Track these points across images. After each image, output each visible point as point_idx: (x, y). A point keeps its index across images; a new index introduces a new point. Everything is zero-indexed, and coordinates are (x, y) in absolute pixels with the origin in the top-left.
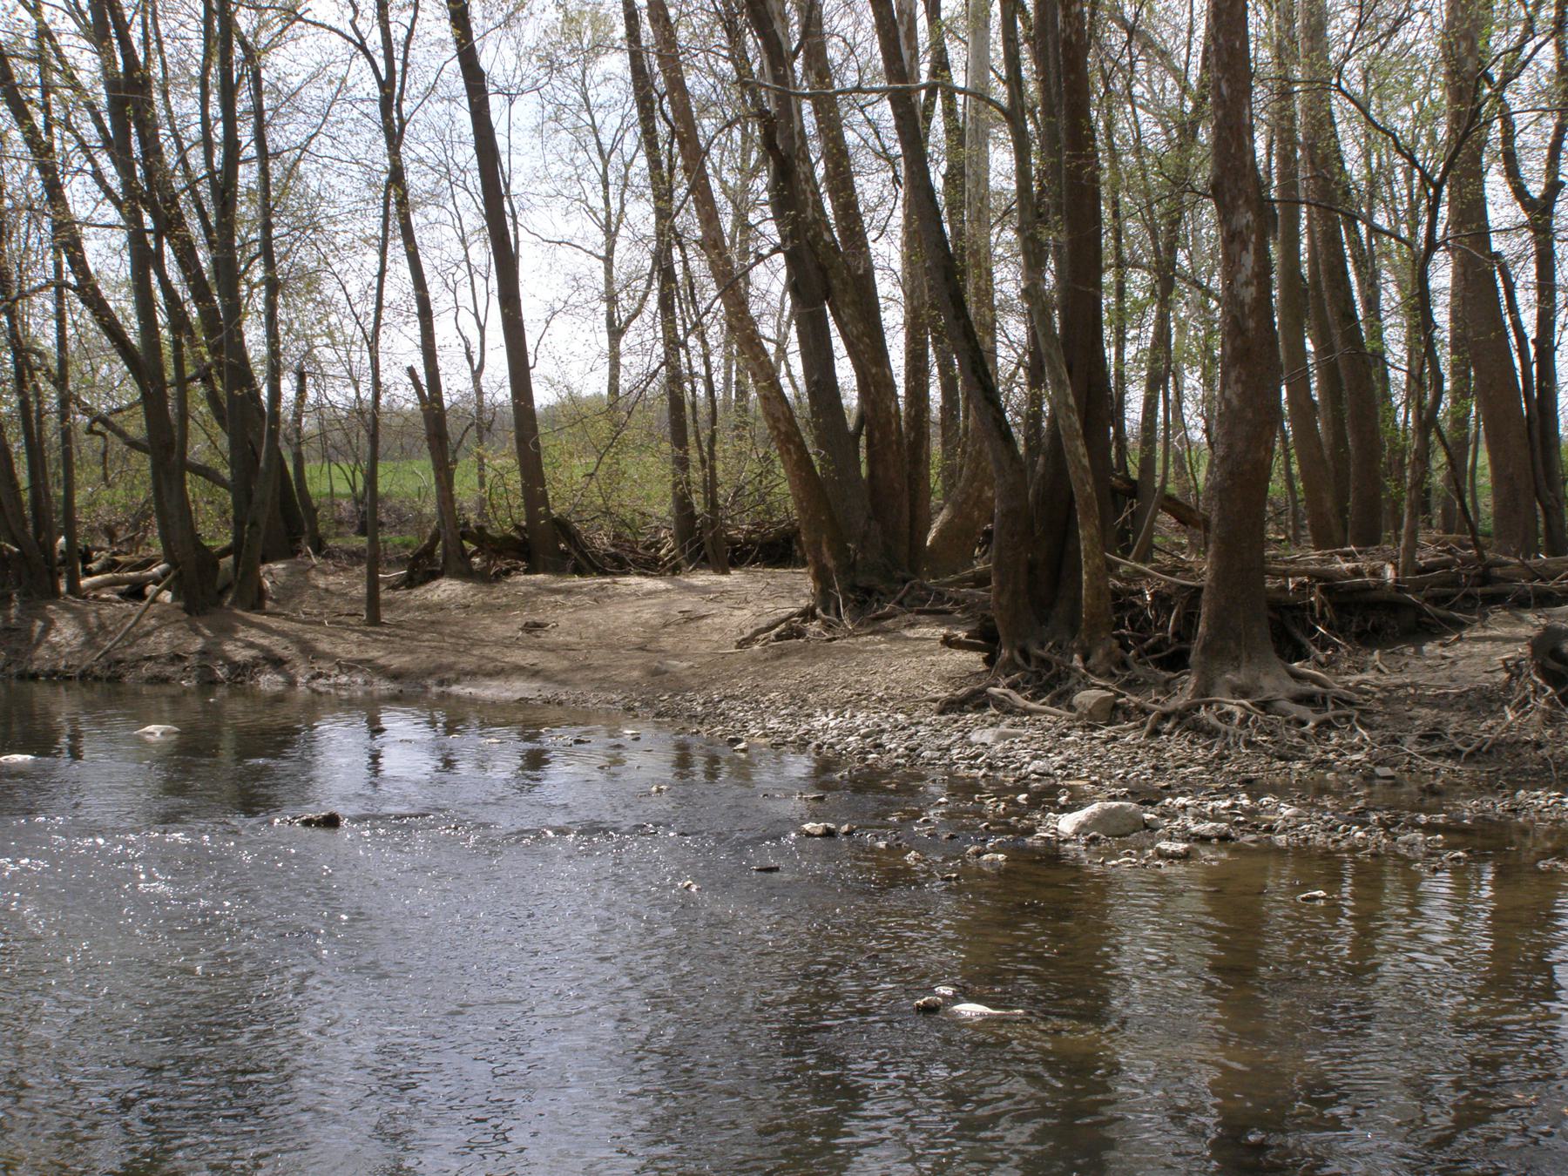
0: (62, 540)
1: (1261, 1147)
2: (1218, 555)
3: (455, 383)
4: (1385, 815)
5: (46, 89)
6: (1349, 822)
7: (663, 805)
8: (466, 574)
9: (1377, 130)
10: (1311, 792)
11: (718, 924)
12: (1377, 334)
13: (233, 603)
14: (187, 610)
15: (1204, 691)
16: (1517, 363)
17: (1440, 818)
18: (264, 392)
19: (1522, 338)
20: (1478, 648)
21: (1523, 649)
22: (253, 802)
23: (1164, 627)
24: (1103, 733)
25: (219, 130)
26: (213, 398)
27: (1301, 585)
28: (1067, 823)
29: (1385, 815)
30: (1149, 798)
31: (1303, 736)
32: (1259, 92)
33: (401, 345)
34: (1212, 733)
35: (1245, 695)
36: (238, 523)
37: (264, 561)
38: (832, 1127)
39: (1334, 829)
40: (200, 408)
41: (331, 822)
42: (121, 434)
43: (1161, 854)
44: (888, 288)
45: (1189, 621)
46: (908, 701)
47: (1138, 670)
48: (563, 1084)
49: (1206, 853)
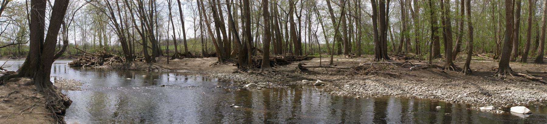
0: (133, 55)
1: (269, 121)
3: (177, 37)
4: (282, 84)
5: (132, 5)
6: (278, 85)
7: (201, 84)
8: (178, 58)
9: (282, 9)
10: (274, 82)
11: (207, 97)
12: (282, 31)
13: (152, 62)
14: (147, 62)
15: (262, 71)
17: (288, 84)
18: (156, 38)
19: (297, 32)
20: (293, 66)
21: (297, 66)
22: (154, 84)
23: (258, 64)
24: (251, 75)
25: (151, 9)
26: (150, 39)
27: (273, 59)
28: (247, 86)
29: (282, 84)
30: (256, 83)
31: (273, 76)
32: (269, 4)
33: (171, 33)
34: (263, 75)
36: (153, 53)
37: (156, 57)
38: (220, 120)
39: (277, 86)
40: (148, 40)
41: (164, 86)
42: (140, 43)
43: (258, 89)
44: (226, 26)
45: (261, 63)
46: (229, 72)
47: (255, 68)
48: (190, 115)
49: (263, 89)
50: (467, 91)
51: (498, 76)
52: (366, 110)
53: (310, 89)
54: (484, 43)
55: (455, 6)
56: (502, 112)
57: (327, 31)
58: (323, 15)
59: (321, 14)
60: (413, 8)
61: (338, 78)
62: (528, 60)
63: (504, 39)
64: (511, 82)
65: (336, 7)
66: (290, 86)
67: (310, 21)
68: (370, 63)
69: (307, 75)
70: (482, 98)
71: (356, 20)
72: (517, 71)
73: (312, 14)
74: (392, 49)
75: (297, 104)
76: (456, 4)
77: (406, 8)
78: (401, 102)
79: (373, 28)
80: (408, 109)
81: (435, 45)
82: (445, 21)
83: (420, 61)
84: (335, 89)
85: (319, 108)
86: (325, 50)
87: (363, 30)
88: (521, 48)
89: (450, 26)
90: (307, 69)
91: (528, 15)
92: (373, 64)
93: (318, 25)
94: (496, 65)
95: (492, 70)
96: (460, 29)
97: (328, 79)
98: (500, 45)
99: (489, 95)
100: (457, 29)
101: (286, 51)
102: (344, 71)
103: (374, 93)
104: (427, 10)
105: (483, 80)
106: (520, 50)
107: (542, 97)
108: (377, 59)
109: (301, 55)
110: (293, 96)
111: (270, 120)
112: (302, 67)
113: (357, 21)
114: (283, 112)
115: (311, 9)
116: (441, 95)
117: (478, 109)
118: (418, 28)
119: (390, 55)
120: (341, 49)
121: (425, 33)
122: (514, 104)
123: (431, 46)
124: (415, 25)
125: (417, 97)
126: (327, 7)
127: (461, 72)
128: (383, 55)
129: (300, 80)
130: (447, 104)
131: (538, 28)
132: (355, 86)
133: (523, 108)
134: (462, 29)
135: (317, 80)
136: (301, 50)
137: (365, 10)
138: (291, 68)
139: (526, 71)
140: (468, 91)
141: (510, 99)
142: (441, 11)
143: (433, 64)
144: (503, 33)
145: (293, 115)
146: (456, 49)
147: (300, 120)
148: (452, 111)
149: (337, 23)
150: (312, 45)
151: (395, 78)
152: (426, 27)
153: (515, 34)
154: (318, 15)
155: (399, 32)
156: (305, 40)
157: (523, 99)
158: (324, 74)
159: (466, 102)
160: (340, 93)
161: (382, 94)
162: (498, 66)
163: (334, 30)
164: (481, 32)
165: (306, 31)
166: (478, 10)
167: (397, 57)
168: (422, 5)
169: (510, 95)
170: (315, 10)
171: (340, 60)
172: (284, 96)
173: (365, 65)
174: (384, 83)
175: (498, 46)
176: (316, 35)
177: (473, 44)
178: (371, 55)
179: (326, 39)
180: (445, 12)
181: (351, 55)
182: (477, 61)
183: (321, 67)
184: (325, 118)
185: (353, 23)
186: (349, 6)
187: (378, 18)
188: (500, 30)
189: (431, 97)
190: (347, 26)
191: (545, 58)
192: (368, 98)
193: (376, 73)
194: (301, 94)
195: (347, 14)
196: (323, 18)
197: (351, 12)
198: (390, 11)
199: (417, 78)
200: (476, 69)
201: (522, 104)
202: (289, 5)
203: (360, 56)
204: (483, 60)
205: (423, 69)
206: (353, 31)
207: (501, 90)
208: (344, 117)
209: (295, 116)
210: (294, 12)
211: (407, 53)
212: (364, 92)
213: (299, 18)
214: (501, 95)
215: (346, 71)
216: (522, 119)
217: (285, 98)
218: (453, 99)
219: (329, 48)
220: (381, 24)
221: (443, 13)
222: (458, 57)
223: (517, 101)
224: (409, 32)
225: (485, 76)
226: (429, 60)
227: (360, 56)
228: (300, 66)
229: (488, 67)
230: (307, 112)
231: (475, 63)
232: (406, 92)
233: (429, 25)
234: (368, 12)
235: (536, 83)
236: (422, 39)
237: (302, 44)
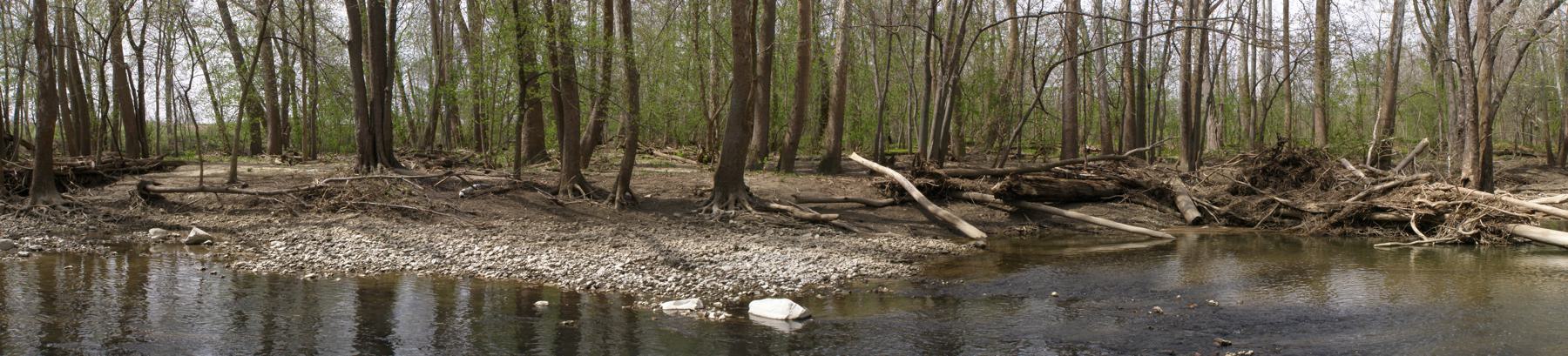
2: (39, 159)
4: (92, 241)
6: (80, 243)
9: (89, 25)
10: (68, 235)
12: (89, 88)
15: (34, 203)
16: (132, 97)
17: (109, 241)
19: (134, 90)
20: (121, 188)
21: (135, 188)
23: (21, 183)
29: (92, 241)
30: (15, 237)
32: (50, 10)
34: (37, 216)
35: (47, 204)
43: (20, 256)
45: (29, 180)
47: (12, 197)
49: (34, 255)
50: (625, 255)
51: (711, 212)
52: (332, 315)
53: (172, 255)
54: (670, 117)
55: (586, 11)
56: (724, 315)
57: (219, 86)
58: (209, 40)
59: (202, 39)
60: (466, 19)
61: (251, 221)
62: (797, 164)
63: (727, 106)
64: (748, 229)
65: (246, 17)
66: (114, 246)
67: (171, 60)
68: (343, 178)
69: (162, 213)
70: (668, 277)
71: (302, 55)
72: (766, 198)
73: (174, 39)
74: (407, 136)
75: (134, 298)
76: (589, 6)
77: (445, 20)
78: (434, 289)
79: (351, 78)
80: (455, 309)
81: (530, 125)
82: (559, 54)
83: (487, 172)
84: (243, 253)
85: (200, 309)
86: (213, 142)
87: (322, 82)
88: (778, 130)
89: (573, 69)
90: (163, 198)
91: (797, 36)
92: (352, 180)
93: (193, 70)
94: (705, 180)
95: (696, 194)
96: (601, 79)
97: (222, 225)
98: (717, 123)
99: (687, 268)
100: (593, 77)
101: (101, 146)
102: (268, 202)
103: (355, 264)
104: (506, 23)
105: (670, 225)
106: (774, 135)
107: (838, 269)
108: (364, 167)
109: (146, 155)
110: (124, 274)
111: (56, 345)
112: (148, 191)
113: (304, 58)
114: (96, 320)
115: (172, 24)
116: (548, 268)
117: (656, 307)
118: (482, 75)
119: (403, 154)
120: (260, 139)
121: (500, 91)
122: (757, 293)
123: (519, 128)
124: (473, 68)
125: (479, 275)
126: (218, 17)
127: (606, 202)
128: (381, 155)
129: (144, 230)
130: (566, 293)
131: (826, 74)
132: (300, 245)
133: (786, 302)
134: (607, 79)
135: (191, 229)
136: (145, 143)
137: (328, 24)
138: (116, 193)
139: (793, 196)
140: (626, 255)
141: (748, 279)
142: (547, 27)
143: (524, 178)
144: (724, 88)
145: (122, 329)
146: (590, 136)
147: (144, 344)
148: (581, 315)
149: (248, 62)
150: (176, 126)
151: (416, 219)
152: (503, 73)
153: (760, 89)
154: (193, 40)
155: (427, 87)
156: (157, 113)
157: (784, 278)
158: (212, 210)
159: (621, 287)
160: (259, 265)
161: (379, 266)
162: (713, 183)
163: (239, 85)
164: (662, 86)
165: (160, 87)
166: (653, 22)
167: (421, 160)
168: (490, 9)
169: (748, 265)
170: (183, 27)
171: (256, 170)
172: (96, 274)
173: (328, 185)
174: (383, 235)
175: (711, 124)
176: (187, 98)
177: (639, 121)
178: (346, 155)
179: (216, 110)
180: (557, 29)
181: (289, 155)
182: (653, 169)
183: (202, 190)
184: (216, 337)
185: (293, 63)
186: (282, 13)
187: (367, 48)
188: (718, 79)
189: (521, 275)
190: (277, 71)
191: (845, 160)
192: (338, 279)
193: (362, 206)
194: (146, 270)
195: (275, 39)
196: (207, 49)
197: (288, 31)
198: (400, 29)
199: (478, 221)
200: (647, 194)
201: (783, 291)
202: (108, 13)
203: (315, 158)
204: (668, 165)
205: (495, 193)
206: (293, 86)
207: (722, 252)
208: (269, 333)
209: (130, 332)
210: (123, 34)
211: (451, 148)
212: (328, 261)
213: (139, 51)
214: (723, 268)
215: (276, 203)
216: (782, 334)
217: (99, 280)
218: (584, 281)
219: (226, 137)
220: (373, 65)
221: (552, 33)
222: (595, 157)
223: (767, 283)
224: (455, 89)
225: (674, 211)
226: (512, 169)
227: (315, 158)
228: (142, 188)
229: (683, 186)
230: (164, 320)
231: (645, 176)
232: (448, 261)
233: (511, 67)
234: (335, 30)
235: (821, 231)
236: (493, 108)
237: (148, 126)
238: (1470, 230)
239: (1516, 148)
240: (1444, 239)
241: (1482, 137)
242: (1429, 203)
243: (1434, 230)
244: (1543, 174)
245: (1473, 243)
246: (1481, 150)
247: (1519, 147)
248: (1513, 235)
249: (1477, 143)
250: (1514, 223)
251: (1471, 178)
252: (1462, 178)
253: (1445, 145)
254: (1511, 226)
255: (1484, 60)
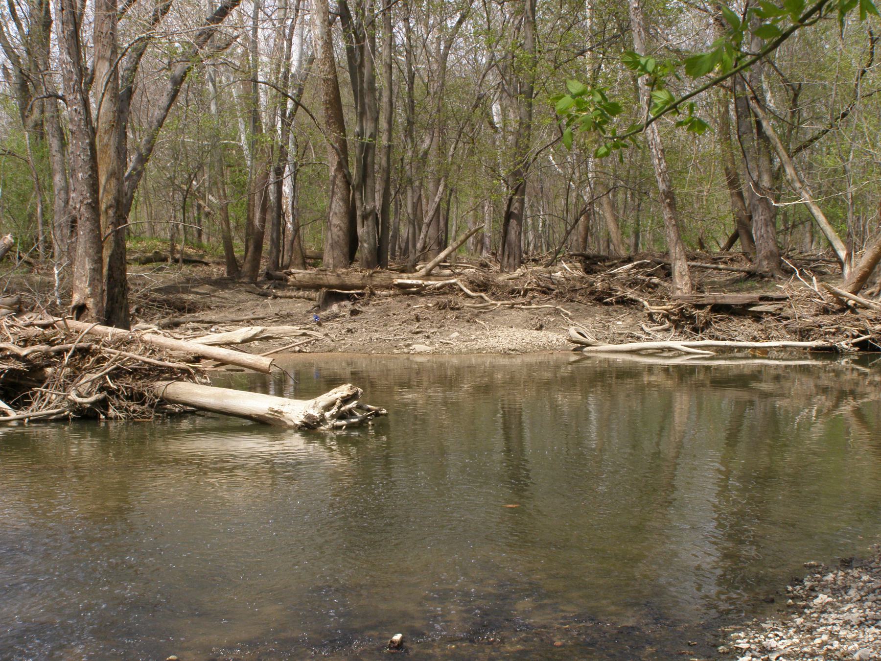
238: (89, 394)
239: (173, 250)
240: (45, 412)
241: (107, 230)
242: (17, 350)
243: (27, 397)
244: (221, 293)
245: (96, 418)
246: (106, 254)
247: (179, 247)
248: (165, 400)
249: (98, 242)
250: (166, 379)
251: (90, 303)
252: (74, 303)
253: (49, 246)
254: (161, 386)
255: (107, 97)
